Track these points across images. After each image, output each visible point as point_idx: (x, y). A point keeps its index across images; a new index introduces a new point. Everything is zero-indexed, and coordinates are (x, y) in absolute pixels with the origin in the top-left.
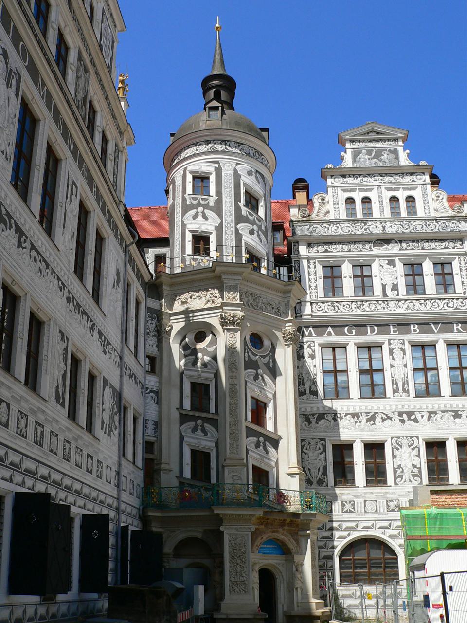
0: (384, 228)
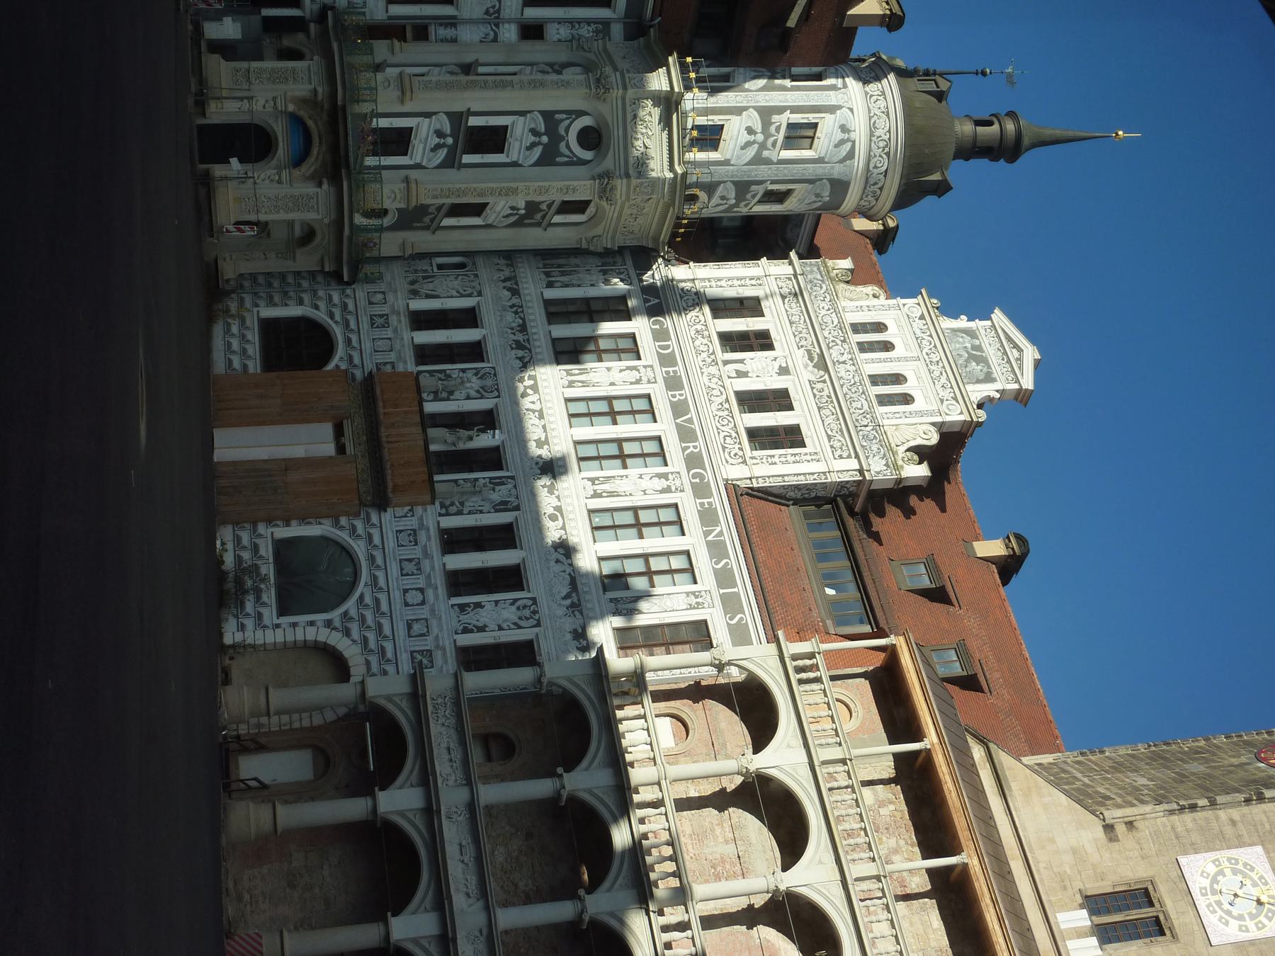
0: (844, 362)
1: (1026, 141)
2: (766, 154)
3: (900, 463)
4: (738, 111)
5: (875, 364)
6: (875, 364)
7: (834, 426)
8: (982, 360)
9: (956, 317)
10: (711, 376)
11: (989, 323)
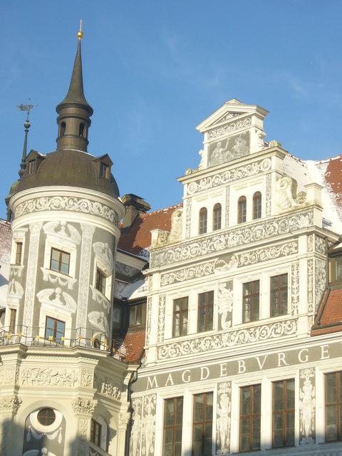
0: (227, 241)
1: (78, 100)
2: (70, 287)
3: (304, 205)
4: (37, 305)
5: (230, 217)
6: (230, 217)
7: (273, 251)
8: (233, 140)
9: (200, 157)
10: (229, 340)
11: (206, 134)
